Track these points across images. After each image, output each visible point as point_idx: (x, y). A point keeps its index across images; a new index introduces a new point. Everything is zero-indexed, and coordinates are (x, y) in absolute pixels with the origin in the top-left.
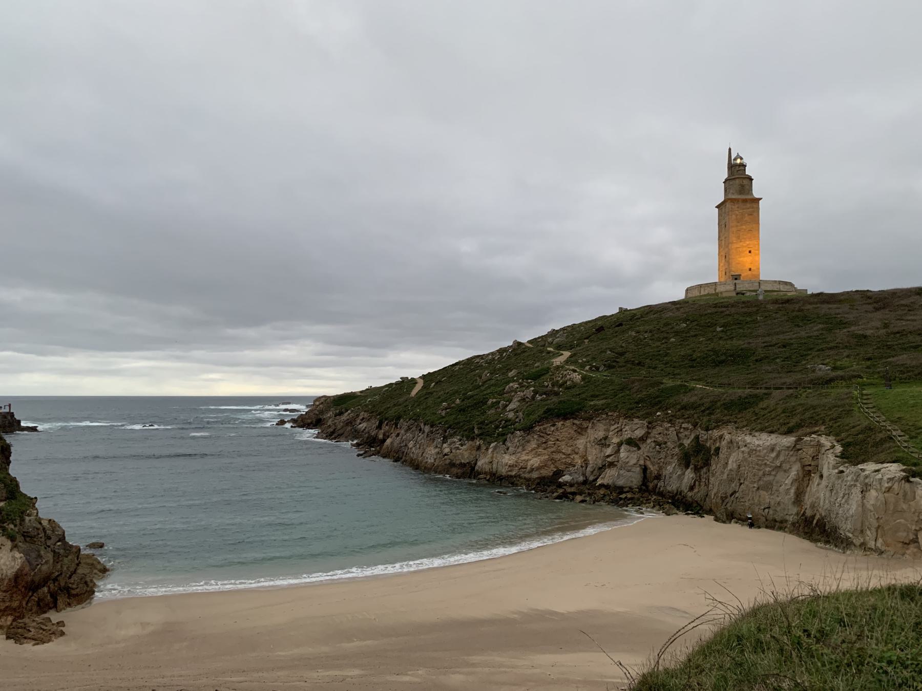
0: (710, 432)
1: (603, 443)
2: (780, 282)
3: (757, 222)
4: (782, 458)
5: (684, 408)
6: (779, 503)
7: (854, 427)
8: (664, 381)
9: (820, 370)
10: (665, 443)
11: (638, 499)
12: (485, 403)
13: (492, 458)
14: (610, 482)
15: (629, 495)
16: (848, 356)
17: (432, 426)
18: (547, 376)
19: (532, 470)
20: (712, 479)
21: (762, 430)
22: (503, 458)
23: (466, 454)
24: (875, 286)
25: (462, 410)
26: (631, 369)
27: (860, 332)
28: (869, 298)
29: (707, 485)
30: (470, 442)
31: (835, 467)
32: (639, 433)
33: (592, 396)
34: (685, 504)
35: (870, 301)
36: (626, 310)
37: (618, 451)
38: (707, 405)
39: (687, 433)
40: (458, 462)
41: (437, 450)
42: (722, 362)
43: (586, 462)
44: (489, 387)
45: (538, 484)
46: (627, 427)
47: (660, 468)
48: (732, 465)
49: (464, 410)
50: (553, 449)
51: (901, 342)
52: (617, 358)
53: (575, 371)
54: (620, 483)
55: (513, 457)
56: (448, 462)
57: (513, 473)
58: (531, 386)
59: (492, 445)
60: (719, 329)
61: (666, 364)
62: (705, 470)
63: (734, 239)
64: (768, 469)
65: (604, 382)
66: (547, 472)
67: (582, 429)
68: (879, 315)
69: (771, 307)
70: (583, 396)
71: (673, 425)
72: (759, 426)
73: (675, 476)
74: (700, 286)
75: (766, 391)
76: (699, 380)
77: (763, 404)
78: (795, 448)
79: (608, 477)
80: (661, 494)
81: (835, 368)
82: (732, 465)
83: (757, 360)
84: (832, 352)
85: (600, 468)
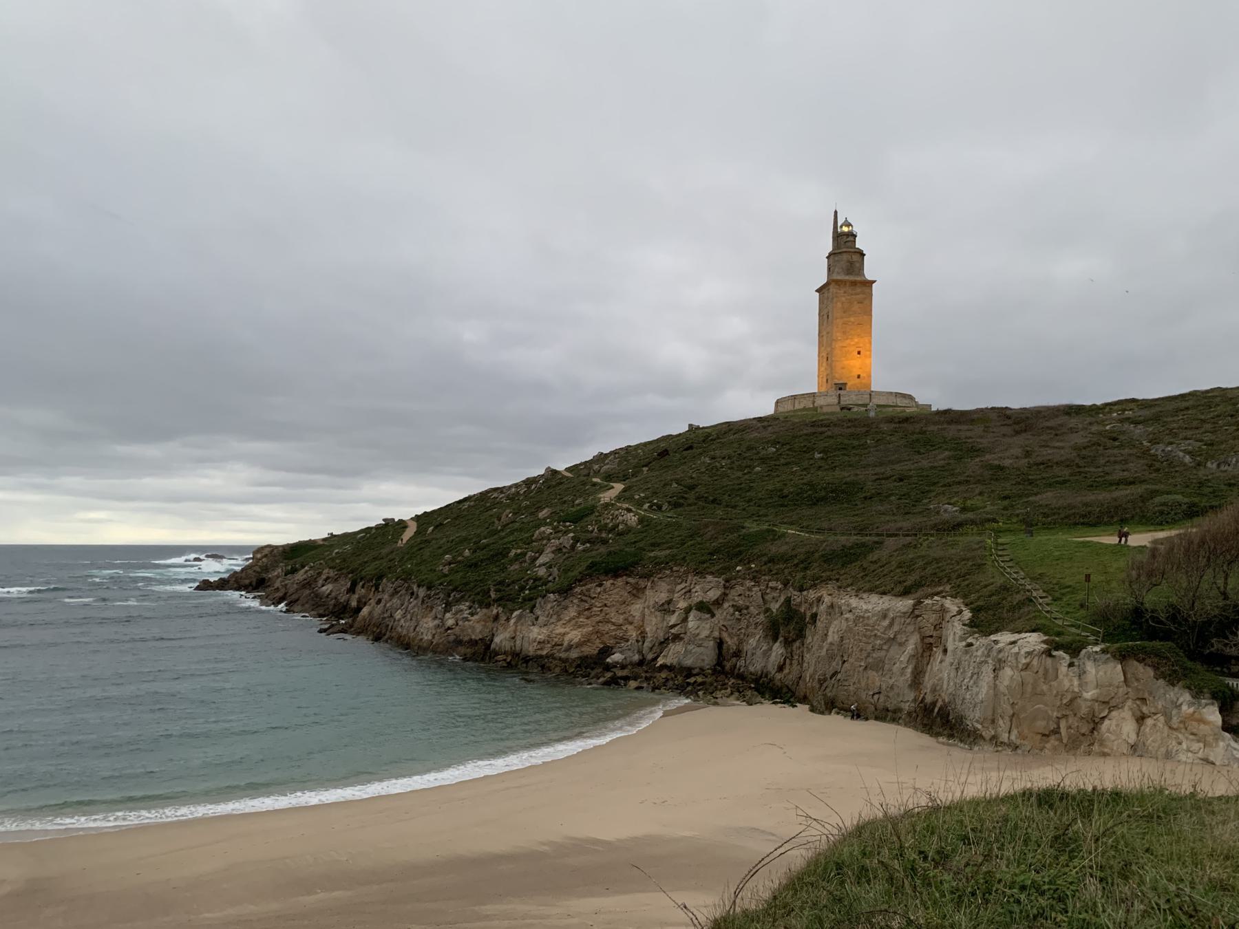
0: (805, 593)
1: (666, 608)
2: (897, 394)
3: (869, 312)
4: (896, 628)
5: (771, 560)
6: (892, 688)
7: (986, 586)
8: (746, 524)
9: (946, 511)
10: (747, 608)
11: (711, 684)
12: (506, 555)
13: (515, 631)
14: (675, 662)
15: (700, 679)
16: (981, 494)
17: (429, 588)
18: (592, 517)
19: (570, 647)
20: (807, 656)
21: (871, 591)
22: (530, 632)
23: (479, 627)
24: (1016, 402)
25: (473, 565)
26: (703, 508)
27: (996, 462)
28: (1009, 417)
29: (801, 664)
30: (485, 610)
31: (962, 639)
32: (713, 594)
33: (653, 545)
34: (771, 689)
35: (1010, 422)
36: (698, 428)
37: (685, 620)
38: (802, 557)
39: (775, 594)
40: (466, 639)
41: (437, 622)
42: (823, 499)
43: (643, 635)
44: (512, 533)
45: (579, 666)
46: (697, 587)
47: (741, 642)
48: (833, 637)
49: (476, 565)
50: (598, 619)
51: (1044, 475)
52: (686, 493)
53: (629, 510)
54: (688, 662)
55: (544, 630)
56: (452, 638)
57: (544, 653)
58: (570, 531)
59: (516, 613)
60: (817, 456)
61: (749, 501)
62: (797, 644)
63: (839, 335)
64: (878, 642)
65: (668, 525)
66: (591, 650)
67: (638, 590)
68: (1020, 440)
69: (885, 427)
70: (641, 545)
71: (758, 583)
72: (868, 586)
73: (759, 652)
74: (794, 397)
75: (876, 539)
76: (792, 523)
77: (871, 557)
78: (913, 614)
79: (673, 655)
80: (741, 677)
81: (964, 510)
82: (833, 637)
83: (865, 498)
84: (962, 488)
85: (661, 643)
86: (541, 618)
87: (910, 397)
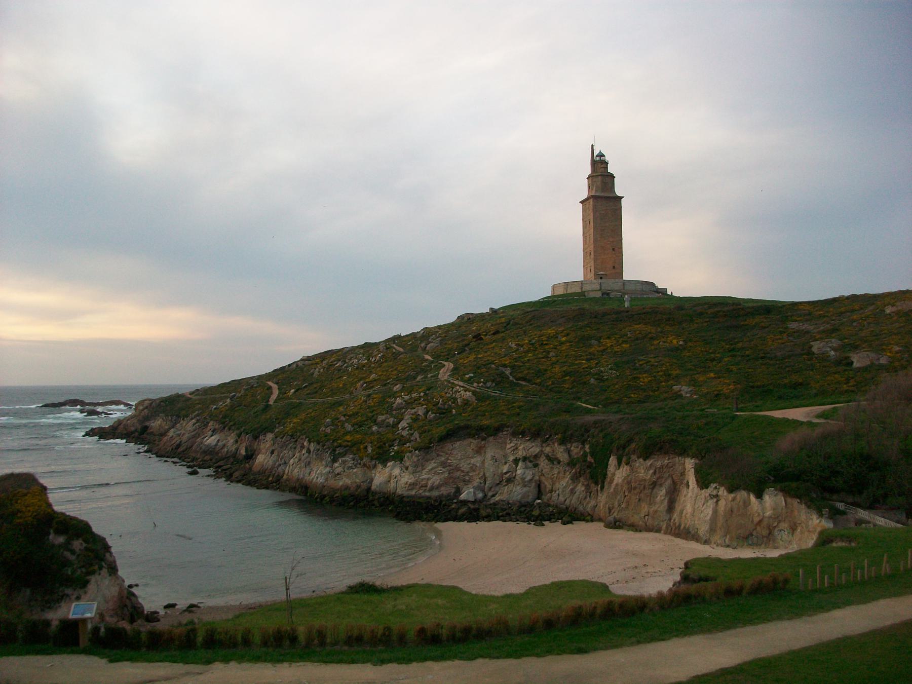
19: (432, 489)
41: (328, 469)
43: (485, 479)
47: (554, 484)
86: (410, 468)
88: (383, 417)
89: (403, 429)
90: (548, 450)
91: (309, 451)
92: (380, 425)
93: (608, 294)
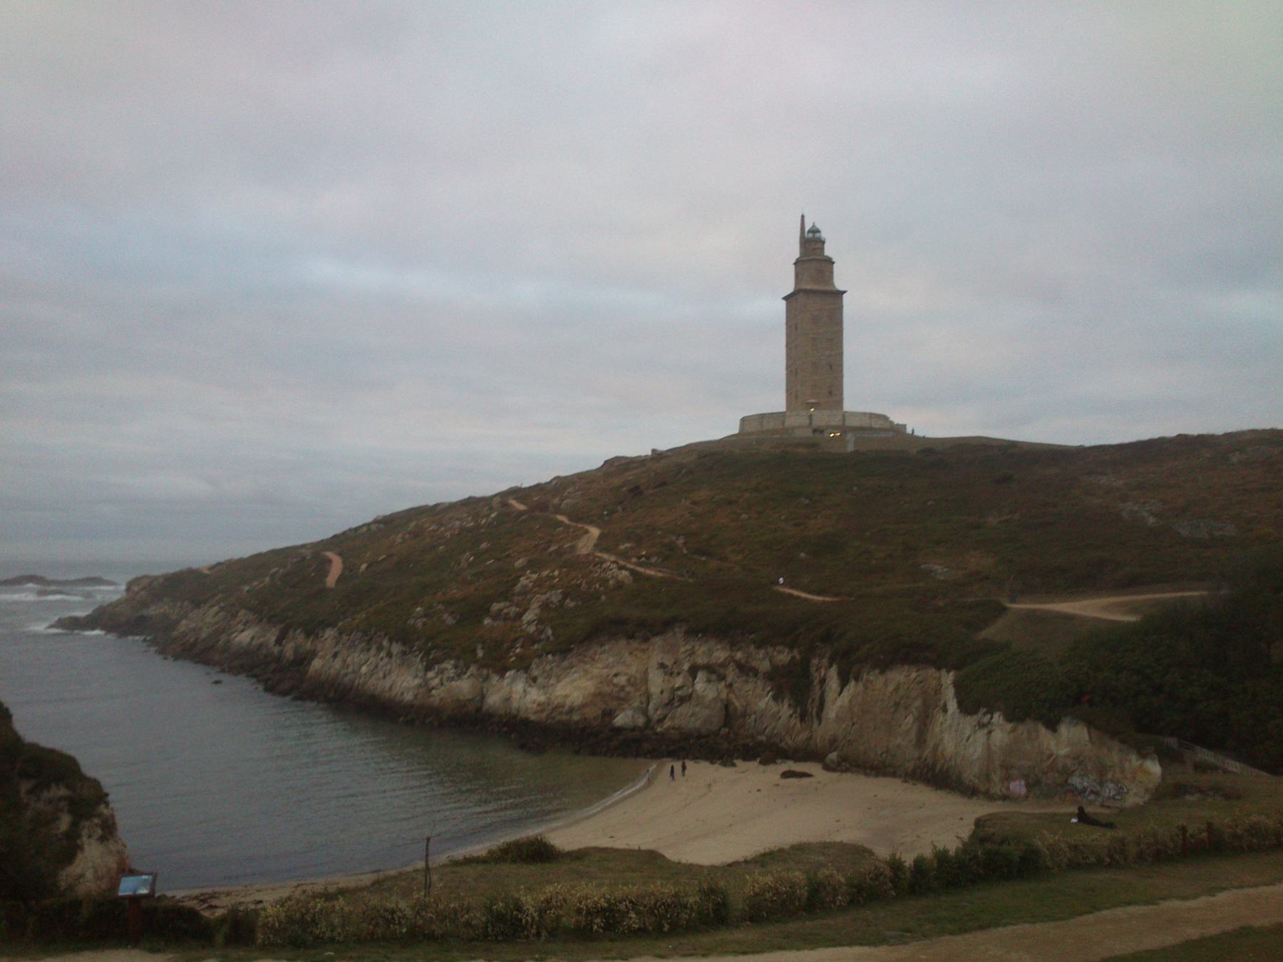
87: (885, 418)
88: (501, 605)
89: (529, 623)
90: (739, 655)
91: (389, 655)
92: (495, 617)
93: (822, 432)
